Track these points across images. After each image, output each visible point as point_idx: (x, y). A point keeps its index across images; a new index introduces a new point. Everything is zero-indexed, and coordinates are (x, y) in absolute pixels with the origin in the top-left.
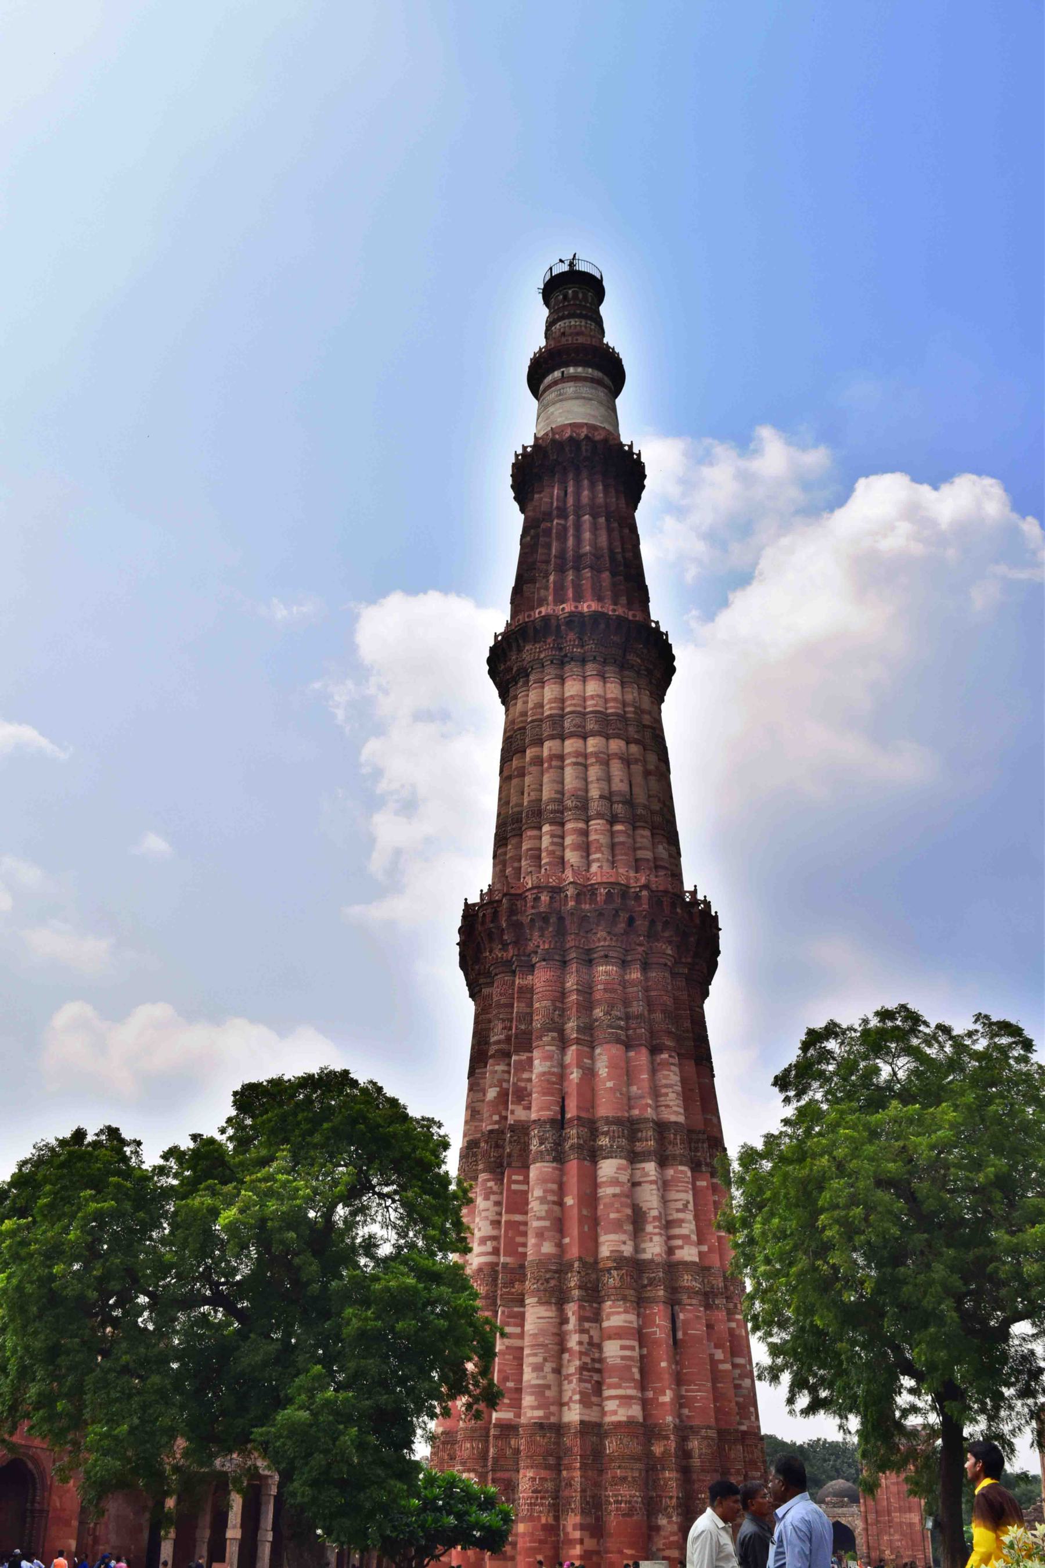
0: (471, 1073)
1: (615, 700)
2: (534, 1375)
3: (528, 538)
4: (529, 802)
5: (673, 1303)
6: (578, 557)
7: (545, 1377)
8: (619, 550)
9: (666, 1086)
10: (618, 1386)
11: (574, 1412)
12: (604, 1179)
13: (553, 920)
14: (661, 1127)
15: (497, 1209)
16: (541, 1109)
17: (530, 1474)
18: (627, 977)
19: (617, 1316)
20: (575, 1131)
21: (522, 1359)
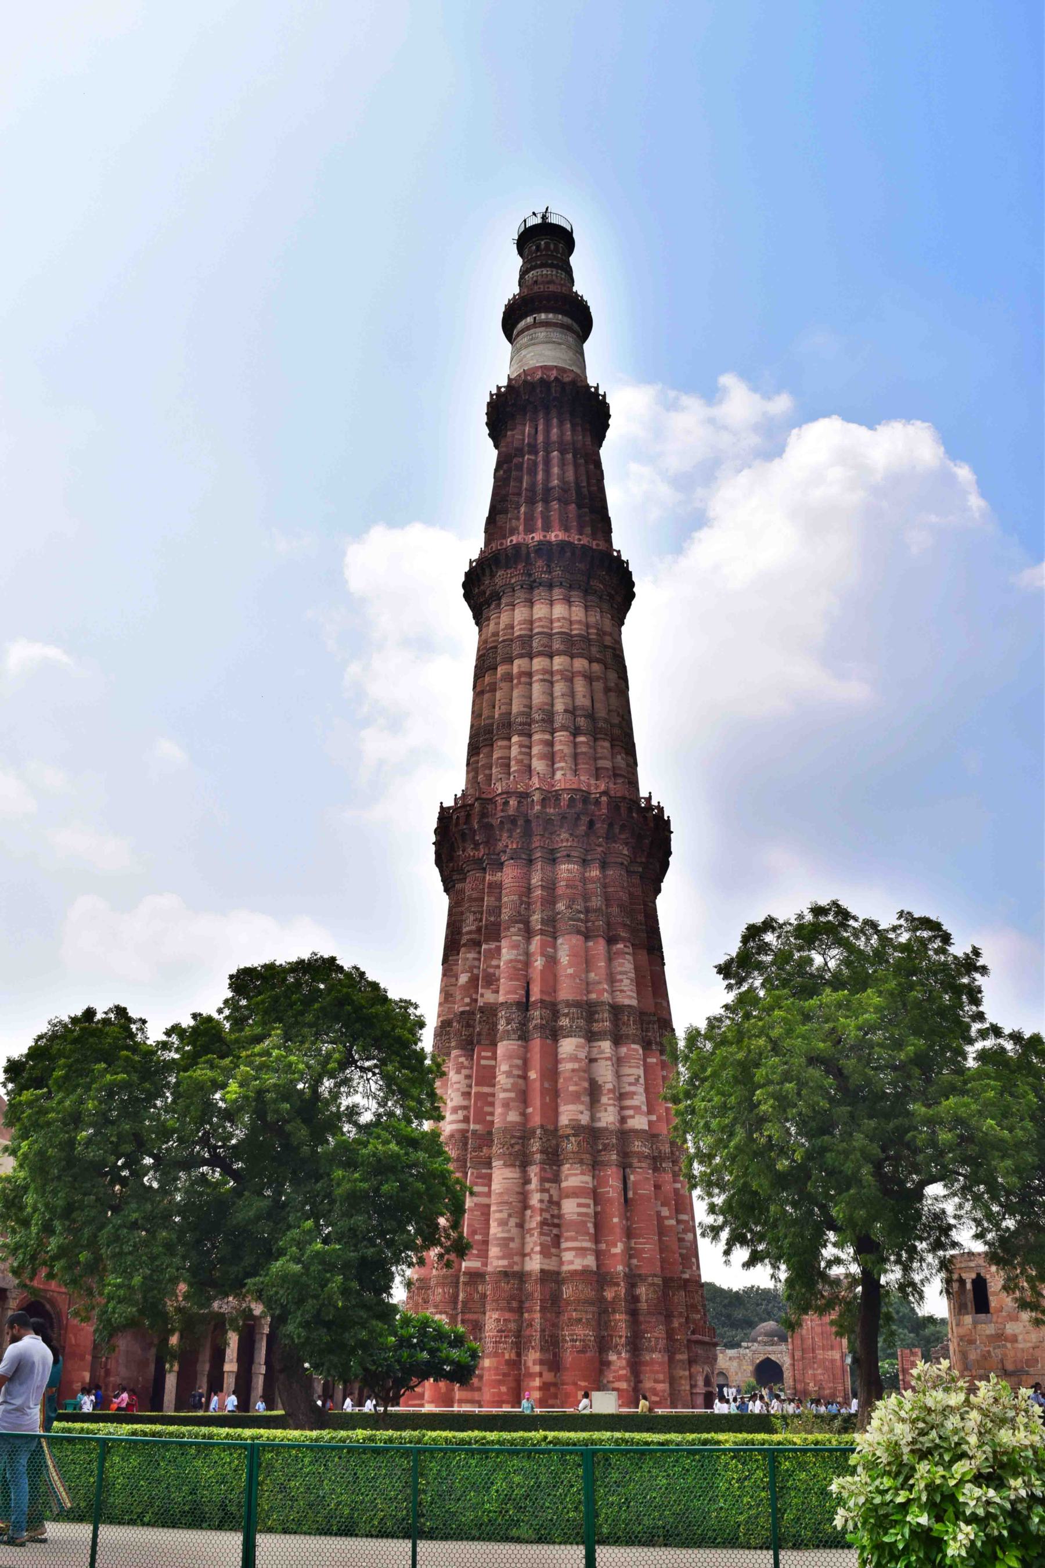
0: (445, 961)
1: (579, 622)
2: (500, 1229)
3: (501, 472)
5: (625, 1166)
6: (547, 490)
7: (509, 1231)
8: (584, 484)
9: (621, 973)
10: (575, 1239)
11: (534, 1262)
12: (564, 1056)
14: (616, 1010)
15: (467, 1081)
17: (495, 1316)
18: (587, 875)
19: (574, 1177)
21: (489, 1214)
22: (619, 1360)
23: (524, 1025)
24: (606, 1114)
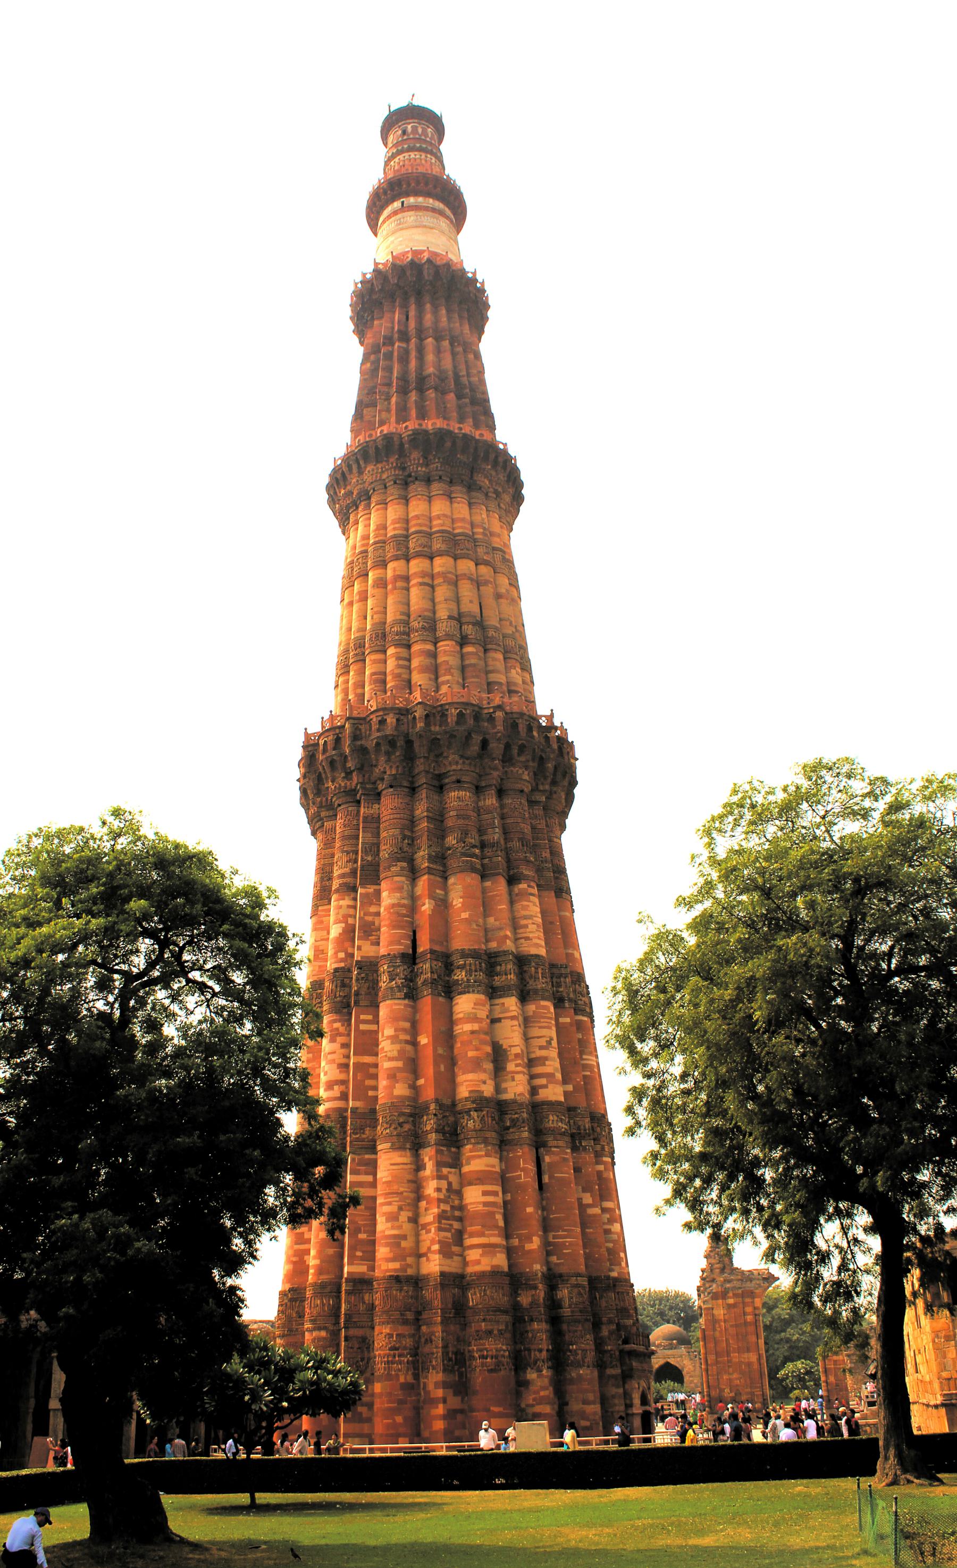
0: (315, 912)
1: (463, 520)
2: (389, 1225)
3: (369, 365)
4: (373, 625)
5: (539, 1145)
7: (400, 1227)
8: (464, 373)
9: (526, 917)
10: (482, 1234)
12: (461, 1015)
13: (400, 743)
14: (522, 961)
15: (343, 1051)
16: (391, 943)
17: (386, 1330)
18: (481, 804)
19: (479, 1160)
20: (428, 965)
21: (374, 1209)
22: (539, 1380)
23: (411, 981)
24: (514, 1083)
